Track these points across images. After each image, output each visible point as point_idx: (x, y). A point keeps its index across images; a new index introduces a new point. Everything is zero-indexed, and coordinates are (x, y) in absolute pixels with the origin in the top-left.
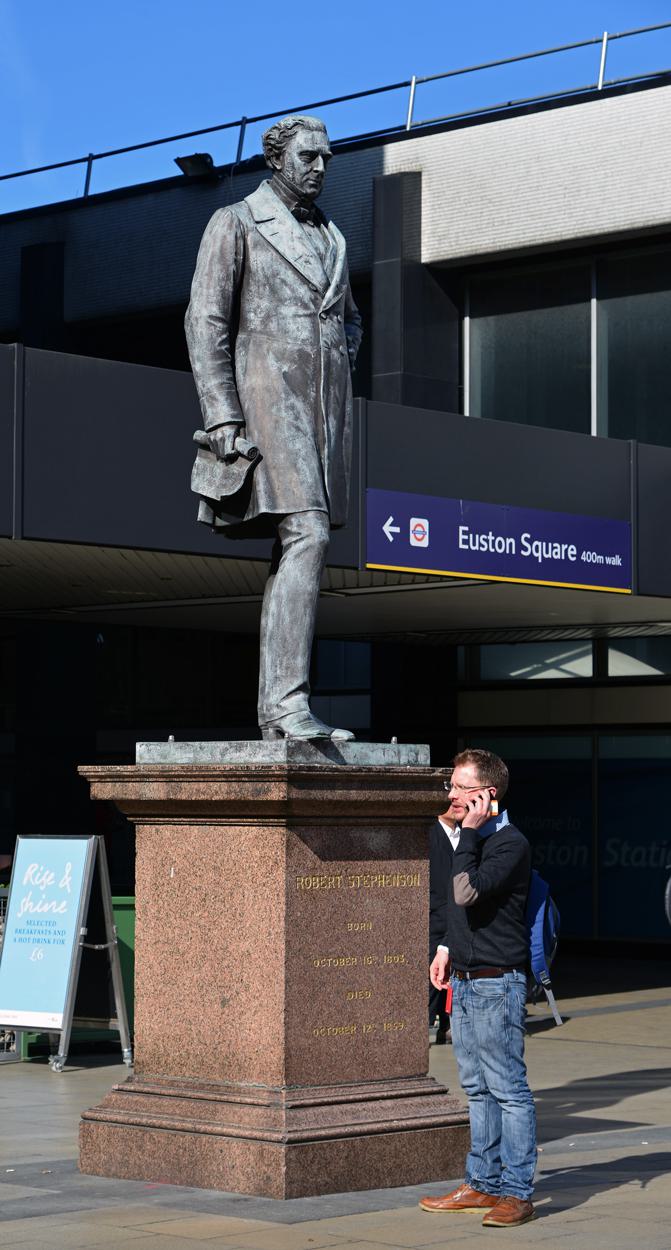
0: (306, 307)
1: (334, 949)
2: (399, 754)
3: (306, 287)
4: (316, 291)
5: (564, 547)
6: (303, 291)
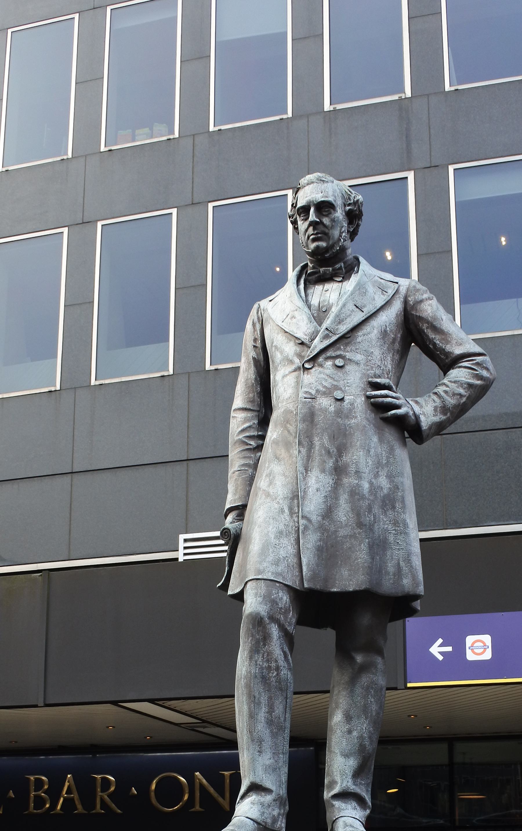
0: (291, 362)
3: (292, 344)
4: (302, 343)
6: (290, 349)
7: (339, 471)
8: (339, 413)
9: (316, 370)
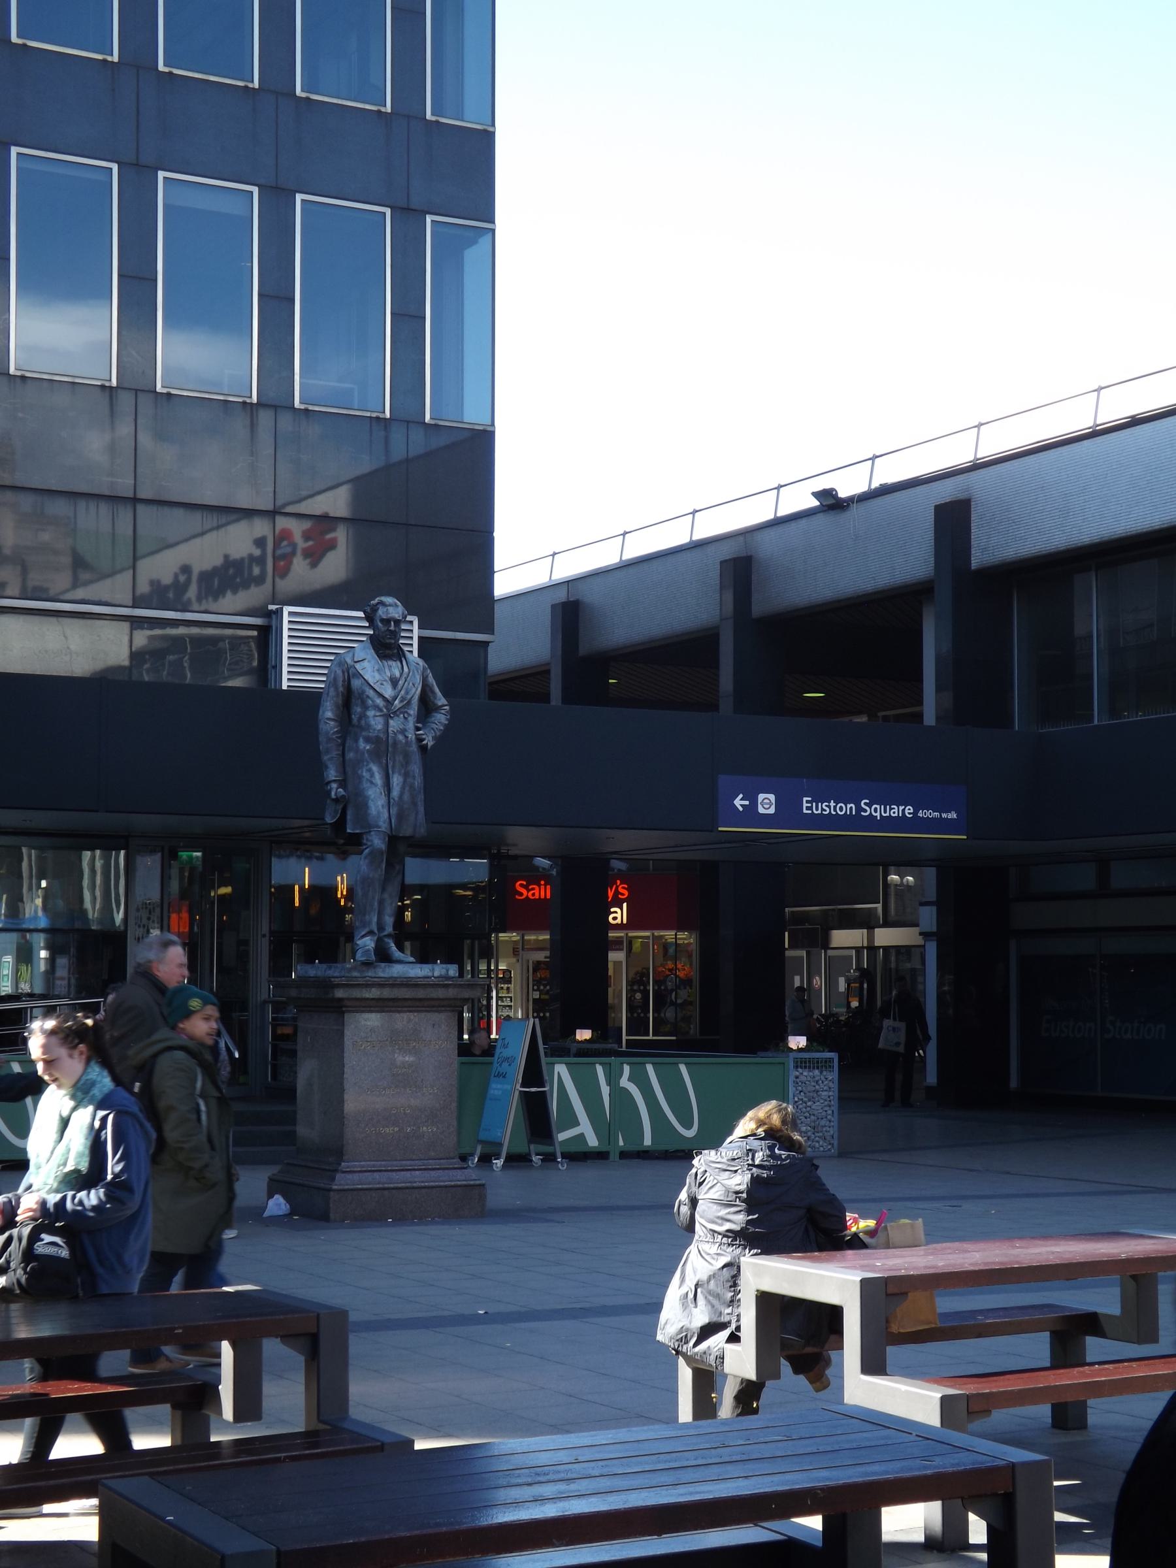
0: (381, 710)
5: (901, 808)
6: (379, 702)
7: (406, 775)
8: (407, 742)
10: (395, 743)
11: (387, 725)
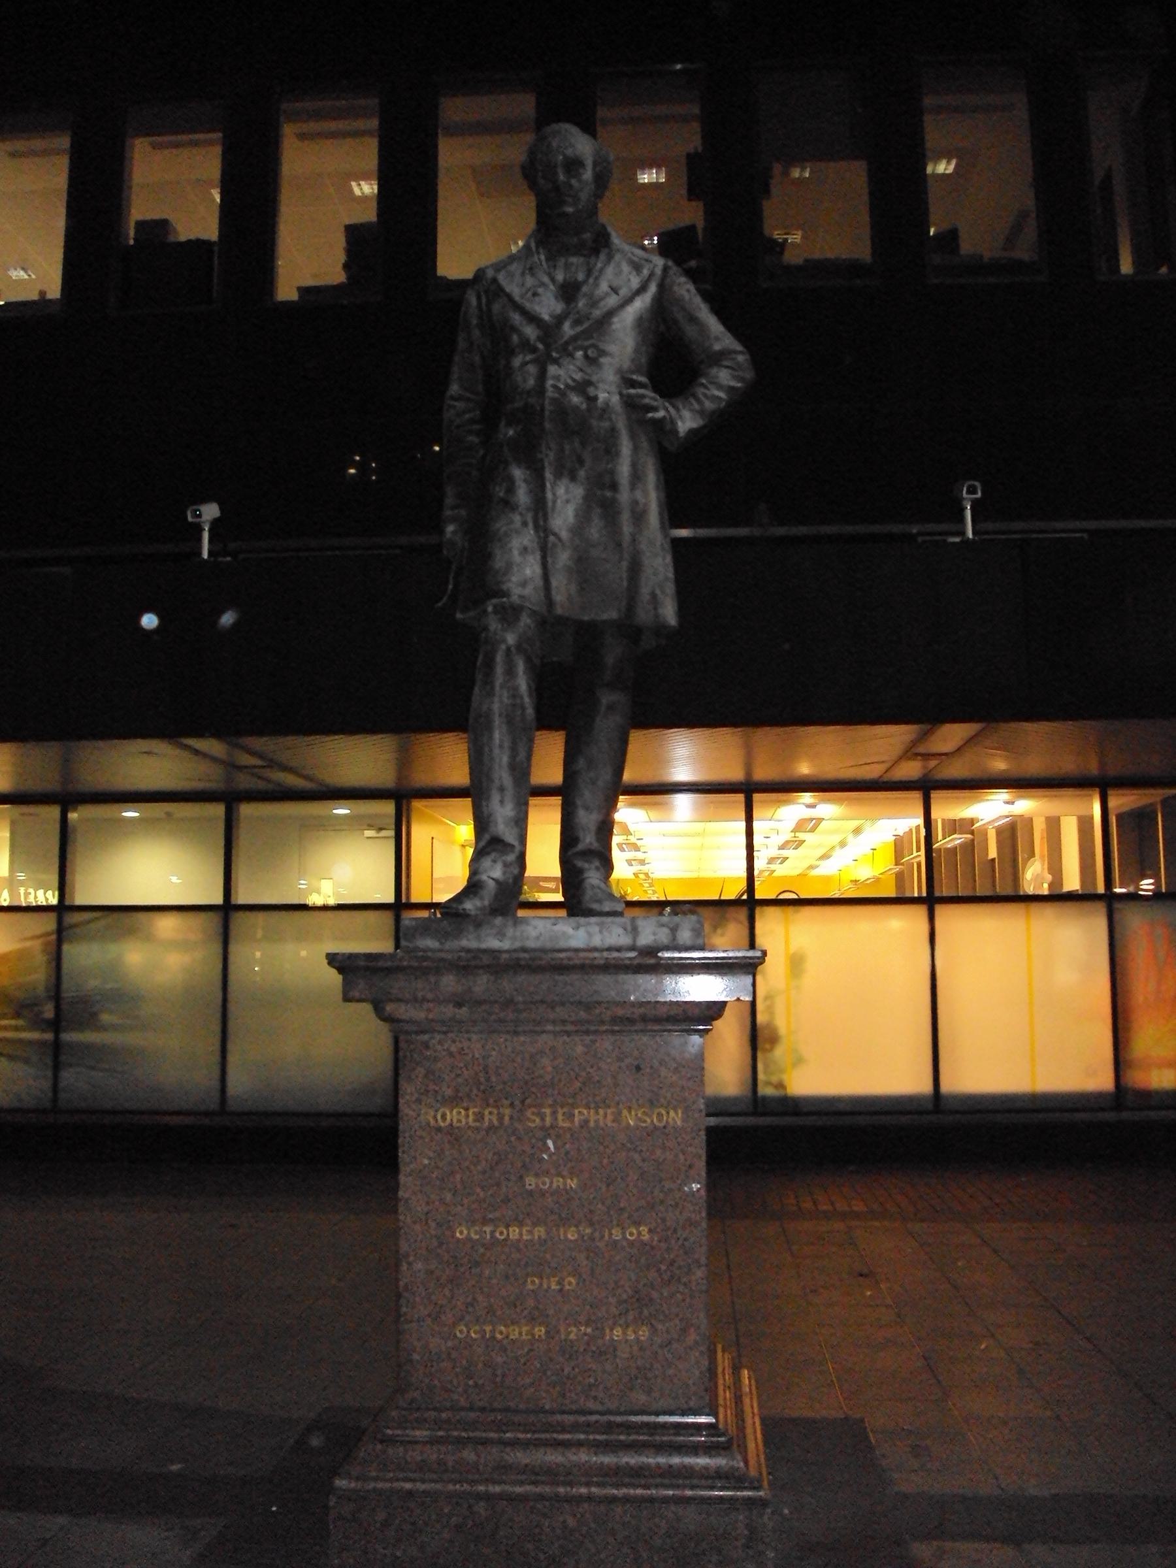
1: (497, 1214)
2: (635, 931)
9: (565, 361)
10: (562, 411)
11: (542, 375)
